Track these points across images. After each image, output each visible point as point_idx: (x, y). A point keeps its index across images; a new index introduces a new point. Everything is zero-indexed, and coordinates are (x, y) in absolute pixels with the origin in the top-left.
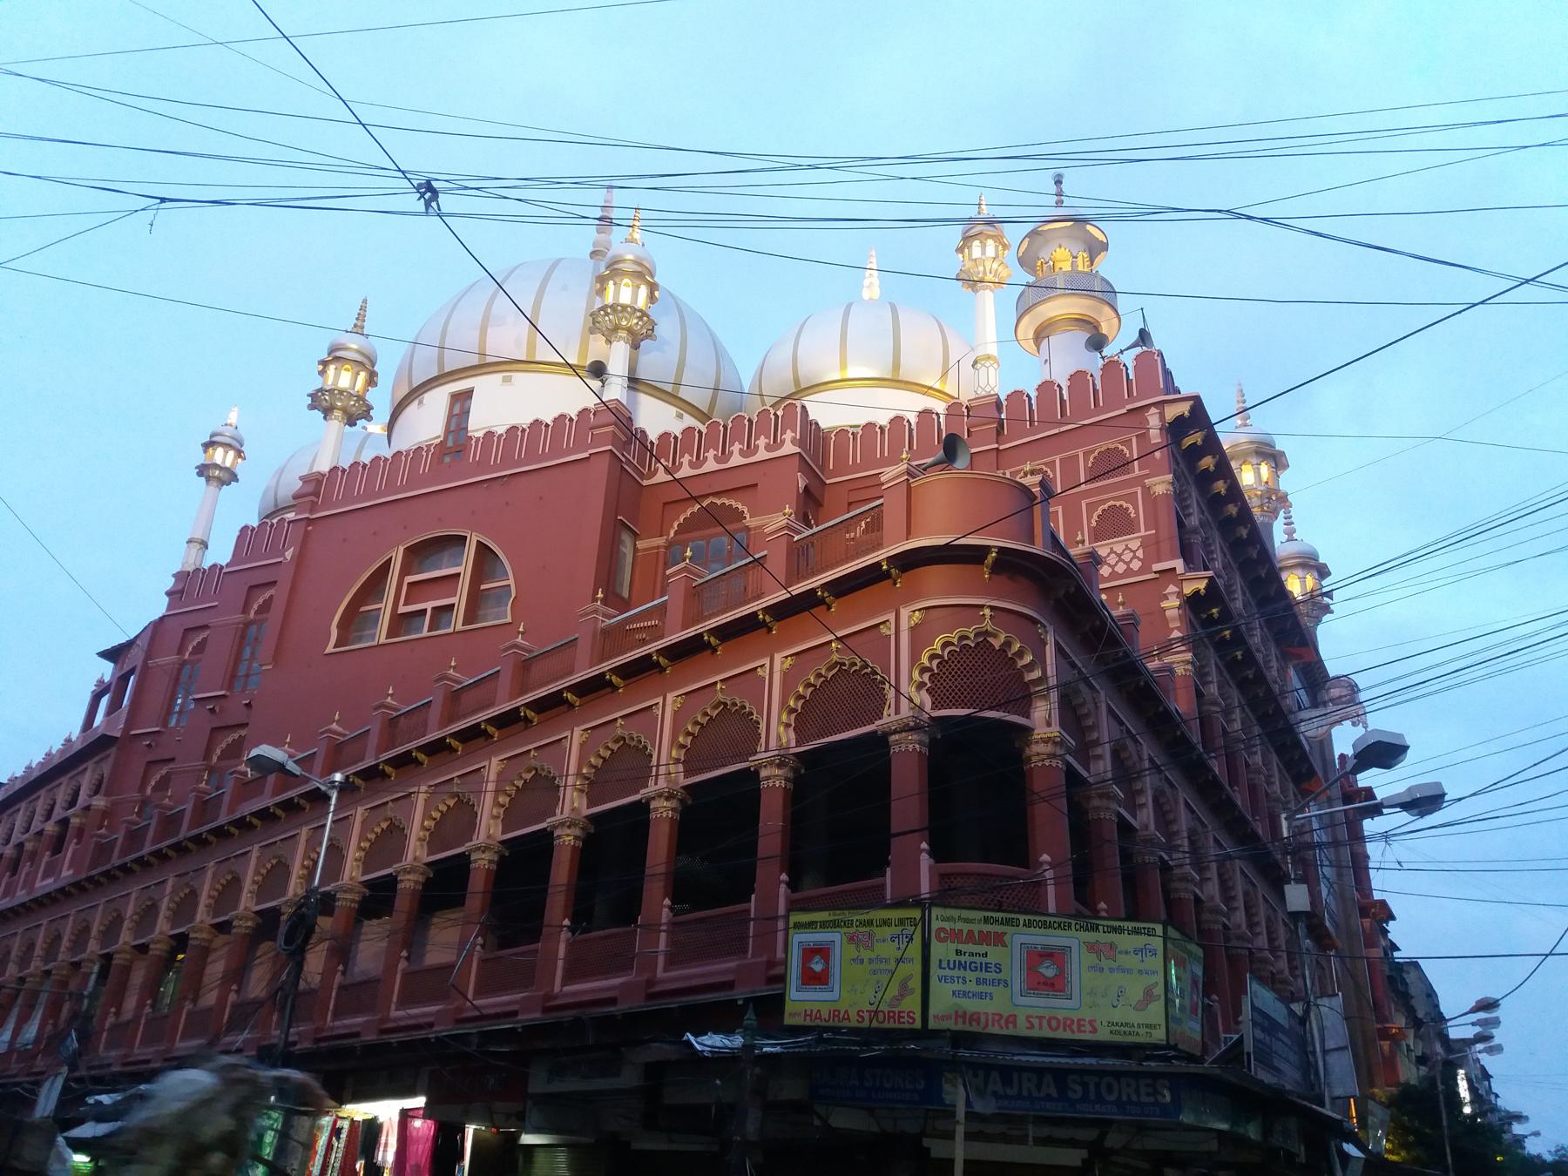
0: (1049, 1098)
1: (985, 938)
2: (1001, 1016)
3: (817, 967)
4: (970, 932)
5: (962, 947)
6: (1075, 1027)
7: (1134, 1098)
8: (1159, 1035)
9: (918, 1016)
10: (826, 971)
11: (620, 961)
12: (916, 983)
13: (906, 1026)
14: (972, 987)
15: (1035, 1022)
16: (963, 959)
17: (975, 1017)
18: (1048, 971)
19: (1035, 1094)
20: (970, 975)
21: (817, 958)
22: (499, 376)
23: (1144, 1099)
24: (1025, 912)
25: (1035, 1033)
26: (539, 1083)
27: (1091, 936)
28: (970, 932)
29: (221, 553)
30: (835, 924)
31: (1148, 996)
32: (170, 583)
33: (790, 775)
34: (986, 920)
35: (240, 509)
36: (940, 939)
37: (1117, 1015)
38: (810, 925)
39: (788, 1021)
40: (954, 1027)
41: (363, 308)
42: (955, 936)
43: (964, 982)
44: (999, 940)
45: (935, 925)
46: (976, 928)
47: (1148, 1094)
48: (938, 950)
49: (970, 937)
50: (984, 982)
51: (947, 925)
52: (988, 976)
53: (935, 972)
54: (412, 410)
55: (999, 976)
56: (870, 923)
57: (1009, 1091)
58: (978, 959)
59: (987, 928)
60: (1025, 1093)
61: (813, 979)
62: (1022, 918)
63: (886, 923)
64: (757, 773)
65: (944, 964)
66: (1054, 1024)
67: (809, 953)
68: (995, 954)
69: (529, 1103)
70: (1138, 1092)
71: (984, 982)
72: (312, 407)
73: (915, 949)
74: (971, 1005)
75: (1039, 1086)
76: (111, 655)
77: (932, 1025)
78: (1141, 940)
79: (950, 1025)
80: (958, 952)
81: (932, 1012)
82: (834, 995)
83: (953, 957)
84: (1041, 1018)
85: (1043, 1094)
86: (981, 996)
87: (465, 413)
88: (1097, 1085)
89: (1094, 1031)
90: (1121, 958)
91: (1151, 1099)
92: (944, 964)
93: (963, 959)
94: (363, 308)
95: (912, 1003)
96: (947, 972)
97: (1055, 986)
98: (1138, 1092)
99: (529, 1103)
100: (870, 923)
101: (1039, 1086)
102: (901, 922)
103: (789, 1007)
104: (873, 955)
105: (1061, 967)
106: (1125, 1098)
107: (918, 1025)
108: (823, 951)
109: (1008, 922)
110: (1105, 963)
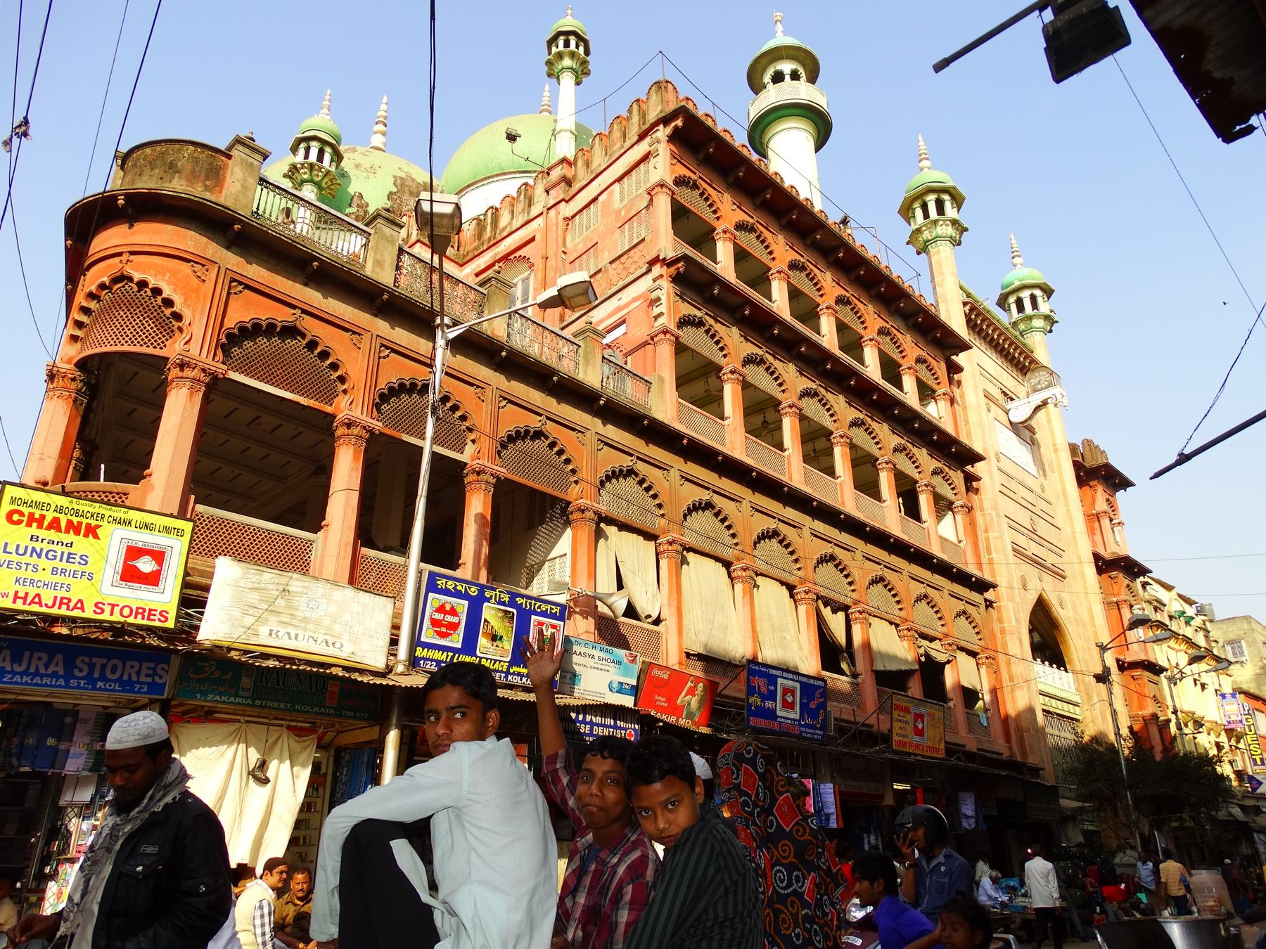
5: (42, 533)
16: (38, 546)
18: (146, 565)
20: (42, 563)
49: (55, 525)
50: (63, 572)
58: (59, 549)
65: (11, 548)
66: (126, 612)
68: (81, 544)
71: (63, 572)
84: (113, 606)
92: (11, 548)
93: (38, 546)
105: (161, 565)
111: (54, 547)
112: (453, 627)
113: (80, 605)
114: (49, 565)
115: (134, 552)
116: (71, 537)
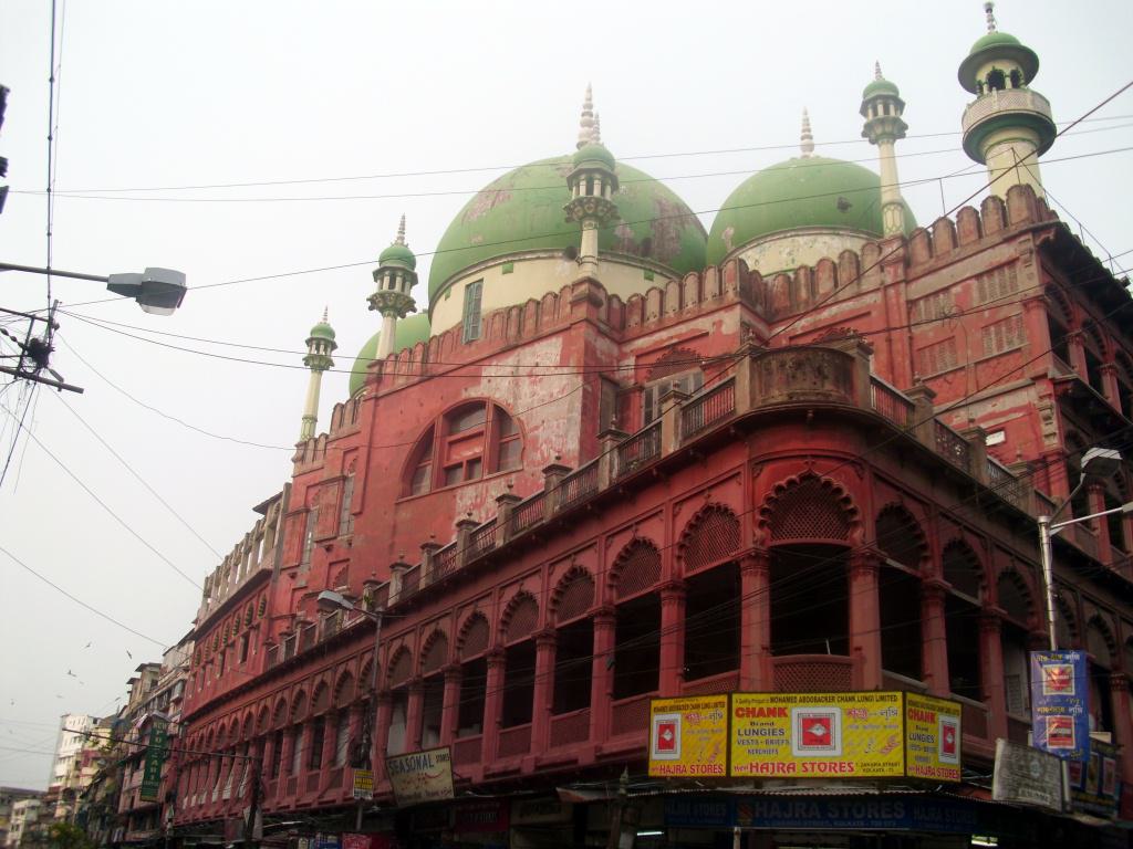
0: (814, 818)
1: (772, 712)
2: (784, 765)
3: (667, 737)
4: (761, 709)
5: (755, 720)
6: (838, 768)
7: (877, 816)
8: (898, 771)
9: (724, 768)
10: (672, 740)
11: (581, 734)
12: (723, 745)
13: (718, 774)
14: (764, 746)
15: (809, 767)
17: (765, 767)
18: (818, 731)
19: (804, 815)
21: (668, 731)
22: (500, 269)
23: (884, 816)
24: (800, 692)
25: (809, 774)
26: (515, 819)
27: (849, 705)
28: (761, 709)
29: (323, 427)
30: (678, 708)
31: (890, 747)
32: (293, 453)
33: (683, 594)
34: (772, 700)
35: (337, 387)
36: (738, 715)
37: (867, 760)
38: (662, 710)
39: (651, 773)
40: (750, 774)
41: (403, 224)
42: (751, 712)
43: (767, 742)
44: (782, 713)
45: (735, 706)
46: (765, 706)
47: (887, 813)
48: (740, 724)
49: (761, 713)
50: (772, 742)
51: (744, 706)
52: (774, 738)
53: (735, 737)
54: (441, 301)
55: (781, 738)
56: (697, 706)
57: (786, 815)
58: (767, 727)
59: (772, 705)
60: (797, 815)
61: (666, 745)
62: (798, 696)
63: (707, 706)
64: (659, 594)
66: (822, 767)
67: (663, 728)
68: (778, 721)
69: (512, 831)
70: (879, 811)
71: (772, 742)
72: (371, 308)
73: (723, 723)
74: (759, 759)
75: (807, 811)
76: (262, 509)
78: (889, 704)
79: (746, 773)
80: (752, 724)
81: (733, 764)
82: (677, 756)
84: (813, 764)
85: (810, 816)
86: (769, 752)
87: (478, 301)
88: (850, 810)
89: (852, 770)
90: (871, 720)
91: (889, 816)
93: (755, 728)
94: (403, 224)
95: (721, 759)
96: (745, 738)
97: (824, 741)
98: (879, 811)
99: (512, 831)
100: (697, 706)
101: (807, 811)
102: (716, 705)
103: (651, 765)
104: (699, 728)
106: (870, 816)
107: (724, 774)
108: (670, 727)
109: (789, 700)
110: (859, 723)
111: (764, 727)
112: (1069, 736)
113: (792, 767)
114: (763, 738)
115: (808, 723)
116: (772, 719)
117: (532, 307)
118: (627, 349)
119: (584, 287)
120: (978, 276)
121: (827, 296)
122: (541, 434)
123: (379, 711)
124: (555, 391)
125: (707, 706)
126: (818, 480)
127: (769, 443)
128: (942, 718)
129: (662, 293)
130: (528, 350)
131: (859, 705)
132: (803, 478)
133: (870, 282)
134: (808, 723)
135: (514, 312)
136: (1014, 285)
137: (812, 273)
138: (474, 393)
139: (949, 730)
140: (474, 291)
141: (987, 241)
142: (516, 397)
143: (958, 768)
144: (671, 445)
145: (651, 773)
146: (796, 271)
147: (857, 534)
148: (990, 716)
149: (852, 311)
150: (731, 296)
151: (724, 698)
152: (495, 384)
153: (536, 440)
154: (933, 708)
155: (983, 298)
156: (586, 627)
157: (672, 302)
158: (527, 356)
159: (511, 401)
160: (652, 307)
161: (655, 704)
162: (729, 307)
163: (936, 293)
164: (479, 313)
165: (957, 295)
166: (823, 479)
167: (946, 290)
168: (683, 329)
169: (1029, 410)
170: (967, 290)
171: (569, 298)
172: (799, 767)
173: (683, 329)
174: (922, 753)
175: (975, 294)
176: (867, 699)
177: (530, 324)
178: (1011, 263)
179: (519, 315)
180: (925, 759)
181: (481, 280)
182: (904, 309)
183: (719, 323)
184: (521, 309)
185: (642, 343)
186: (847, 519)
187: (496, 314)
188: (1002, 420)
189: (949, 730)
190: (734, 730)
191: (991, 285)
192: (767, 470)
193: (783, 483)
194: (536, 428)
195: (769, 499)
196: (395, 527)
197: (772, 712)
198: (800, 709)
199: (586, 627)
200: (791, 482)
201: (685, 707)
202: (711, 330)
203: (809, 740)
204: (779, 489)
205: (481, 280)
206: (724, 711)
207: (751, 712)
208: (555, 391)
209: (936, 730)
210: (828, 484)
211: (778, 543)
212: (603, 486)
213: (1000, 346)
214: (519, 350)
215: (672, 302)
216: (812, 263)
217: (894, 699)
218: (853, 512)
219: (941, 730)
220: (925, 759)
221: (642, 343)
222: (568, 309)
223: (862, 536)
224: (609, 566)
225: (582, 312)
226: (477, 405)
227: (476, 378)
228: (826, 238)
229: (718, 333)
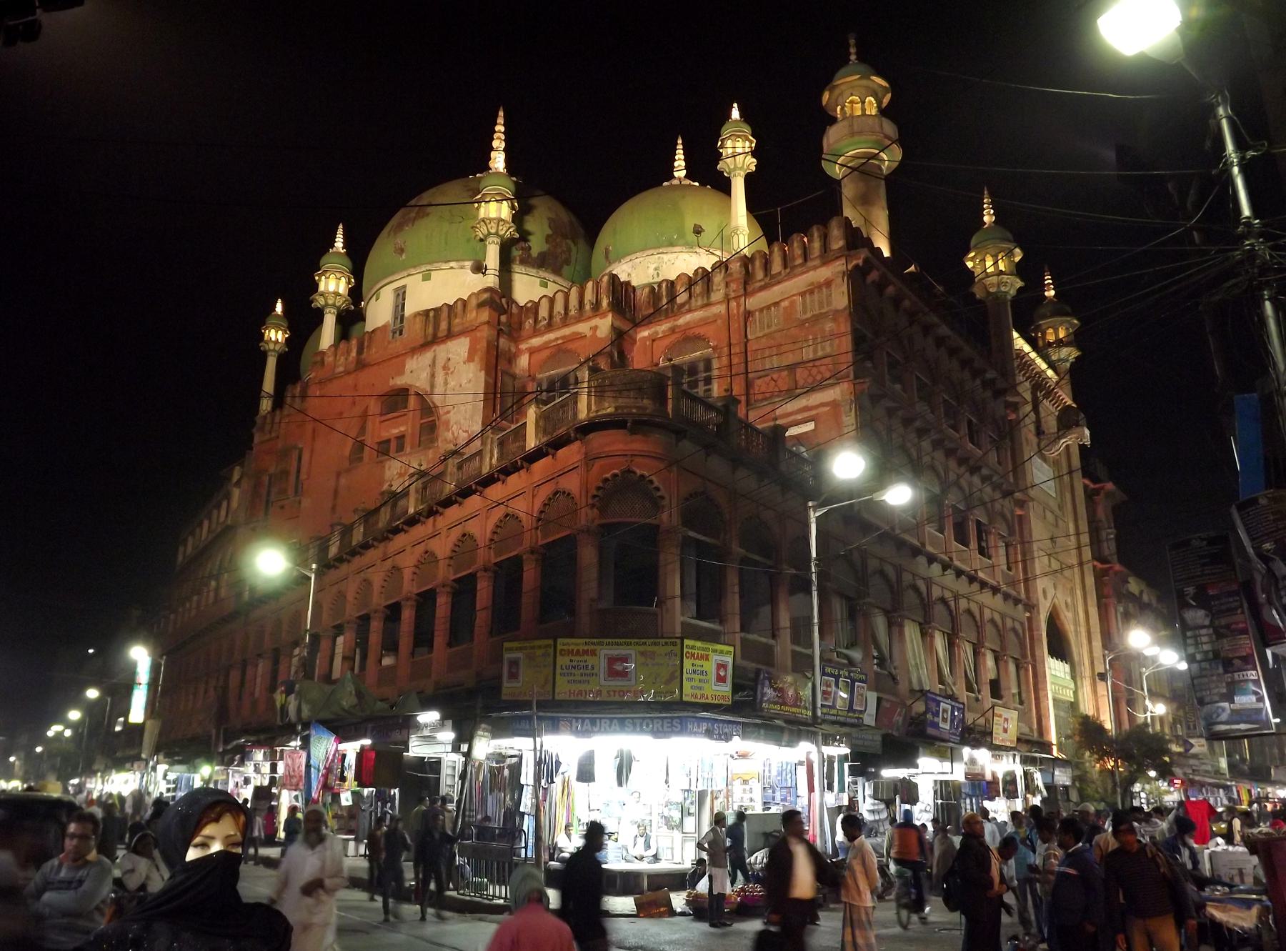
1: (586, 652)
12: (551, 678)
20: (576, 671)
27: (641, 648)
38: (510, 649)
39: (504, 697)
42: (570, 652)
44: (594, 653)
45: (559, 647)
46: (581, 648)
53: (558, 671)
62: (605, 641)
63: (540, 647)
68: (591, 661)
73: (551, 659)
77: (557, 698)
78: (672, 647)
81: (557, 691)
83: (569, 663)
86: (584, 682)
100: (533, 648)
103: (504, 691)
115: (612, 660)
117: (445, 309)
118: (523, 346)
119: (486, 296)
120: (802, 294)
121: (683, 305)
122: (453, 417)
123: (261, 665)
124: (464, 382)
125: (540, 647)
126: (634, 473)
127: (598, 440)
128: (715, 658)
129: (552, 301)
130: (442, 347)
131: (650, 649)
132: (623, 472)
133: (717, 296)
134: (612, 660)
135: (431, 314)
136: (829, 303)
137: (672, 284)
138: (400, 381)
139: (721, 666)
140: (401, 294)
141: (810, 264)
142: (432, 386)
143: (730, 694)
144: (531, 442)
145: (504, 697)
146: (660, 284)
147: (665, 516)
148: (778, 649)
149: (701, 320)
150: (605, 303)
151: (551, 642)
152: (415, 373)
153: (447, 422)
154: (707, 649)
155: (805, 312)
156: (472, 578)
157: (559, 307)
158: (442, 351)
159: (428, 389)
160: (543, 312)
161: (506, 645)
162: (603, 315)
163: (768, 307)
164: (402, 316)
165: (785, 308)
166: (639, 472)
167: (776, 304)
168: (566, 331)
169: (834, 405)
170: (793, 304)
171: (474, 302)
172: (604, 693)
173: (566, 331)
174: (696, 683)
175: (799, 308)
176: (655, 644)
177: (444, 325)
178: (828, 283)
179: (435, 316)
180: (700, 688)
181: (405, 287)
182: (742, 319)
183: (595, 328)
184: (437, 311)
185: (536, 341)
186: (656, 504)
187: (418, 314)
188: (813, 413)
189: (721, 666)
190: (558, 667)
191: (812, 301)
192: (598, 463)
193: (608, 475)
194: (448, 412)
195: (599, 488)
196: (336, 492)
197: (586, 652)
198: (606, 650)
199: (472, 578)
200: (615, 475)
201: (525, 648)
202: (589, 334)
203: (613, 674)
204: (606, 480)
205: (405, 287)
206: (551, 651)
207: (570, 652)
208: (464, 382)
209: (710, 667)
210: (642, 476)
211: (604, 521)
212: (486, 470)
213: (815, 351)
214: (435, 347)
215: (559, 307)
216: (673, 277)
217: (674, 644)
218: (662, 498)
219: (714, 667)
220: (700, 688)
221: (536, 341)
222: (474, 314)
223: (669, 517)
224: (488, 531)
225: (485, 315)
226: (403, 392)
227: (401, 371)
228: (685, 256)
229: (594, 335)
